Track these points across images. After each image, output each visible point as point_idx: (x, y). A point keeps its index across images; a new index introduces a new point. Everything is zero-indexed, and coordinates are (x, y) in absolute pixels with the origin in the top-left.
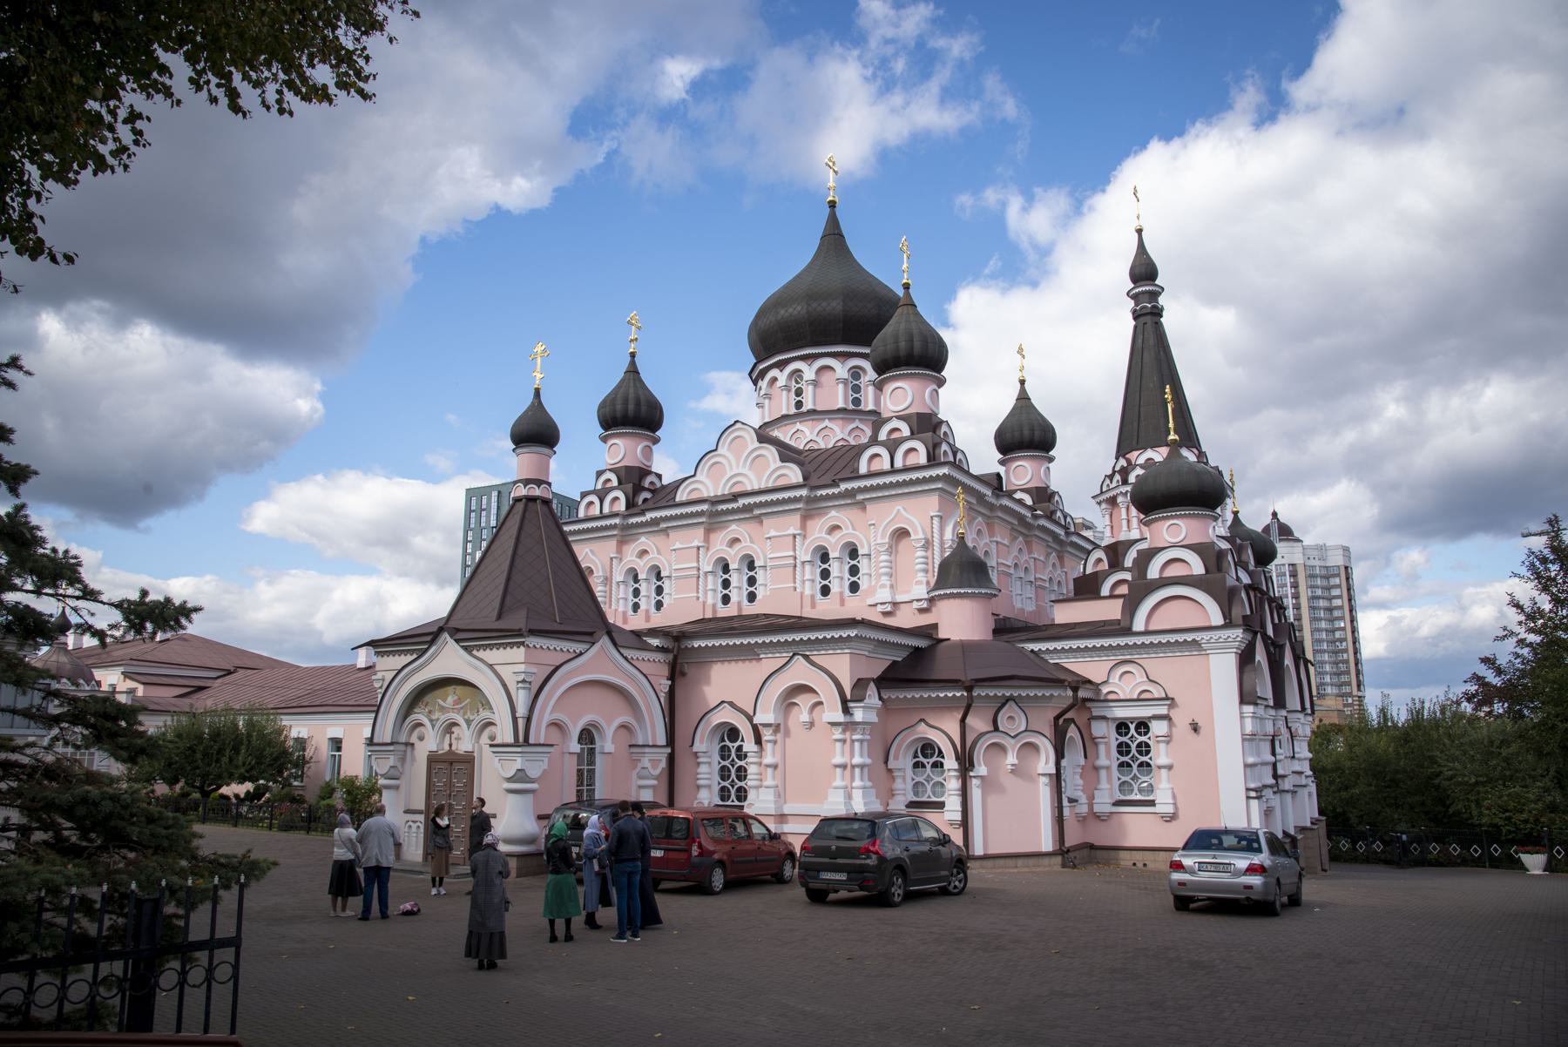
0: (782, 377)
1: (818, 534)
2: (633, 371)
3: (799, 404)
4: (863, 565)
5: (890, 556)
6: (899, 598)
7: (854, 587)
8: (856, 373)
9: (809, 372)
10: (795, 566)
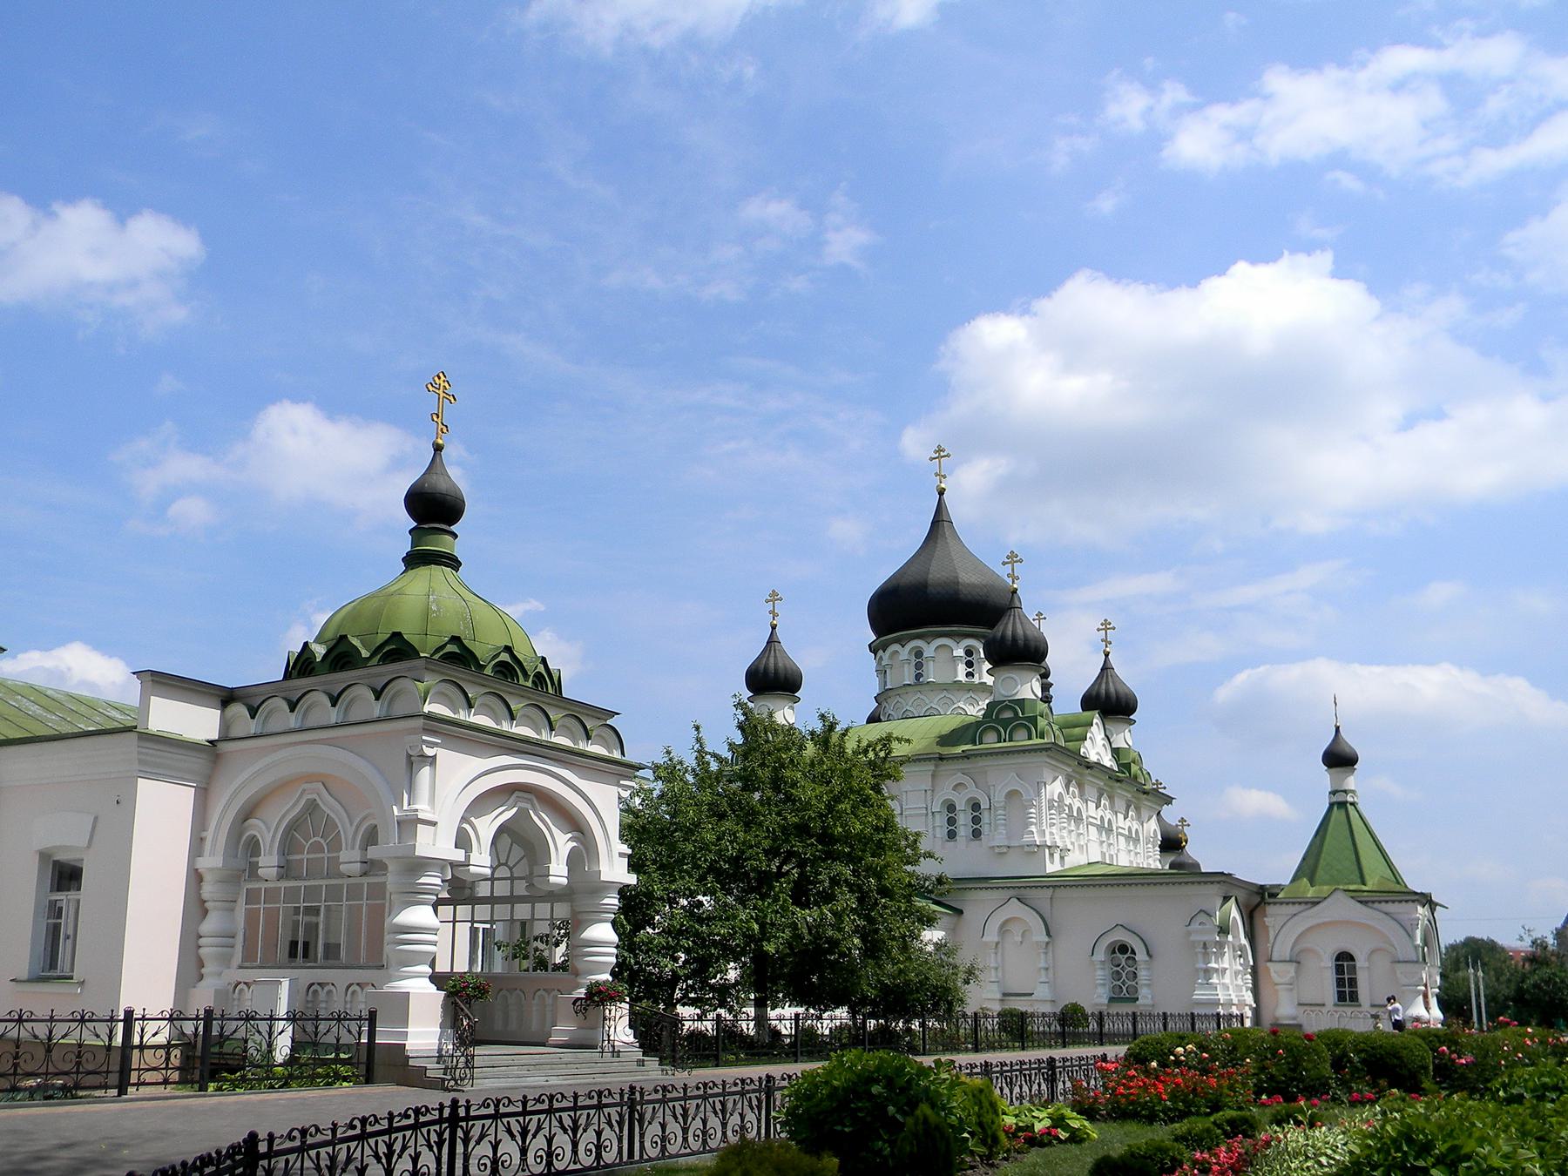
0: (904, 652)
1: (946, 792)
4: (985, 818)
5: (1004, 810)
6: (1013, 844)
7: (977, 834)
8: (969, 652)
9: (929, 649)
10: (927, 814)
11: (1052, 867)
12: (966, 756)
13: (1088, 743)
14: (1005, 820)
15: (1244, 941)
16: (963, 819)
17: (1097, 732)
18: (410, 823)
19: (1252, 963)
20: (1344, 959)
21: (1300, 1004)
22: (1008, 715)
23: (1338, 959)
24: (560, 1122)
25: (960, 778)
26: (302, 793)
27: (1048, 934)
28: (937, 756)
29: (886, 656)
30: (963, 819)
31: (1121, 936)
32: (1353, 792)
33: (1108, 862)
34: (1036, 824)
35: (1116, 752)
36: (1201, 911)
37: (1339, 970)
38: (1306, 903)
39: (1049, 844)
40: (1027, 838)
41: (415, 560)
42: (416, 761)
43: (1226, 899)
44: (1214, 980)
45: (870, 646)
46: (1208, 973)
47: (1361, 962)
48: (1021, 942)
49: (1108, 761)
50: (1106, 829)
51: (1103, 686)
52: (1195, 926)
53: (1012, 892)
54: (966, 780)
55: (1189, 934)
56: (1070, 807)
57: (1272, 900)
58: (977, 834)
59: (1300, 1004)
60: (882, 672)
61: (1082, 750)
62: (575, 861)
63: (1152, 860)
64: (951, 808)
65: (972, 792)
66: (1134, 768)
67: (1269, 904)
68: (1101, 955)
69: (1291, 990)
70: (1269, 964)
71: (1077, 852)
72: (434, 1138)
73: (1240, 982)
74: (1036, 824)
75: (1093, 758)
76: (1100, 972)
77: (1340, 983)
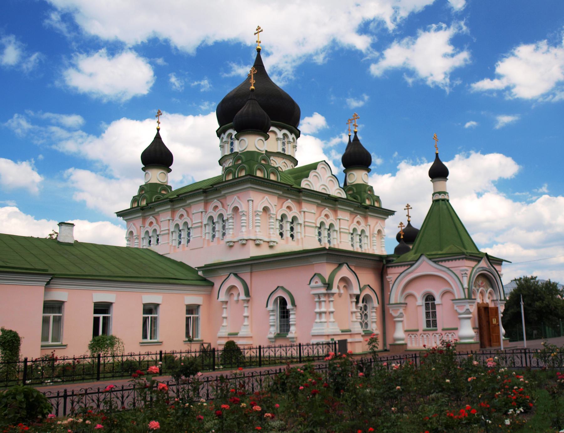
1: (211, 212)
2: (158, 138)
10: (201, 227)
14: (233, 225)
20: (429, 298)
23: (426, 300)
28: (202, 190)
31: (280, 293)
34: (246, 226)
36: (315, 275)
38: (407, 265)
43: (340, 265)
47: (437, 301)
52: (313, 284)
59: (406, 331)
67: (389, 267)
68: (271, 307)
70: (388, 306)
74: (246, 226)
76: (272, 318)
77: (427, 314)
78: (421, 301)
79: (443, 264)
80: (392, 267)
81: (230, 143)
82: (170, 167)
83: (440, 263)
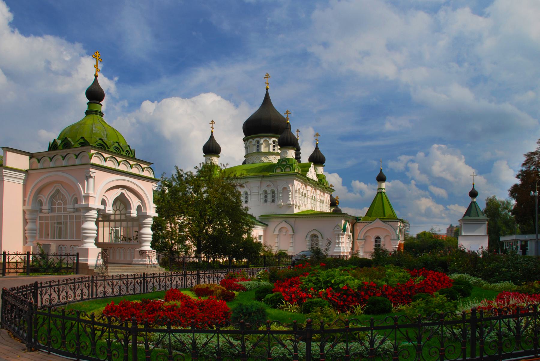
0: (254, 142)
1: (264, 187)
3: (258, 150)
7: (273, 201)
11: (296, 211)
12: (271, 176)
13: (309, 173)
15: (350, 234)
16: (269, 196)
17: (312, 168)
18: (87, 197)
19: (352, 240)
20: (378, 238)
21: (365, 252)
22: (284, 163)
23: (376, 239)
24: (123, 282)
25: (269, 183)
26: (55, 187)
27: (293, 232)
29: (248, 143)
30: (269, 196)
31: (315, 232)
32: (384, 189)
33: (313, 210)
35: (318, 175)
37: (376, 242)
39: (295, 204)
40: (288, 203)
41: (88, 113)
42: (88, 177)
44: (340, 245)
45: (243, 139)
46: (339, 243)
48: (285, 234)
49: (315, 179)
50: (314, 199)
51: (315, 154)
52: (336, 229)
53: (283, 219)
54: (271, 184)
55: (334, 231)
56: (302, 193)
57: (359, 221)
58: (273, 201)
59: (365, 252)
60: (246, 148)
61: (307, 175)
62: (139, 208)
63: (327, 209)
64: (266, 192)
65: (272, 187)
66: (323, 180)
67: (358, 222)
68: (308, 238)
69: (362, 248)
70: (357, 240)
71: (304, 207)
72: (87, 285)
73: (348, 246)
75: (310, 177)
76: (308, 243)
78: (373, 240)
79: (388, 223)
80: (360, 222)
81: (256, 145)
82: (219, 155)
83: (386, 223)
